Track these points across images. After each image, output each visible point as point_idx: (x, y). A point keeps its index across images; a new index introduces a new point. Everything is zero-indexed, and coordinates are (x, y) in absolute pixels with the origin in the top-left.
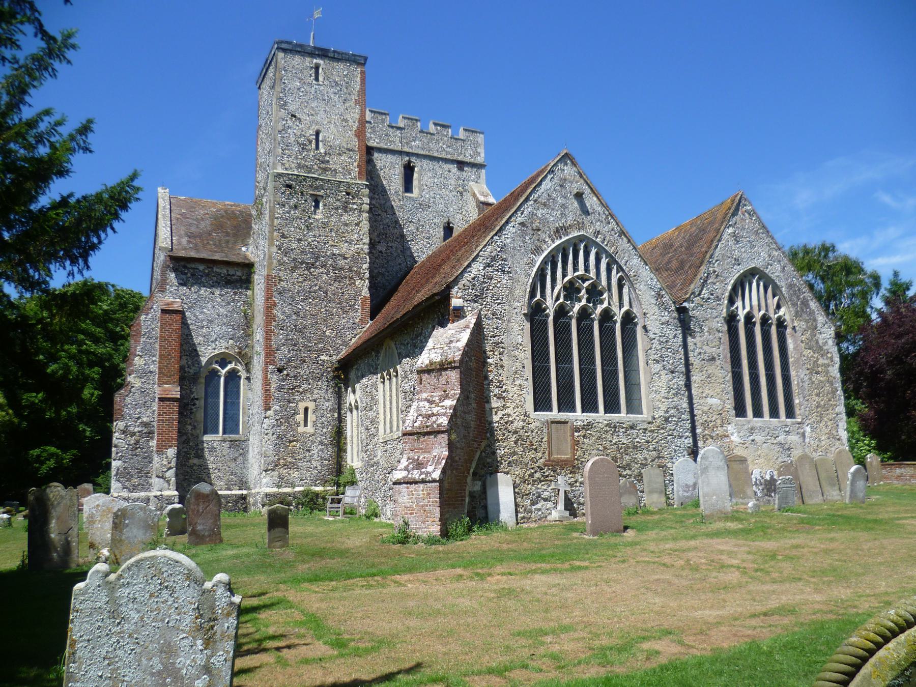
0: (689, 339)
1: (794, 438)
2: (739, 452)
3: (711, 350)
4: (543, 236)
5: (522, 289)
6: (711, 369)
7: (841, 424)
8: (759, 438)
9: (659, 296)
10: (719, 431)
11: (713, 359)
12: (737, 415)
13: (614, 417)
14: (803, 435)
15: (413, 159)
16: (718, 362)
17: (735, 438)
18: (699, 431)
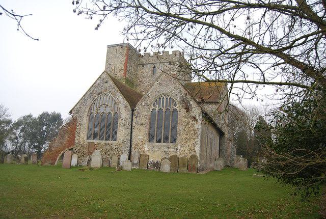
0: (134, 119)
1: (172, 150)
2: (147, 153)
3: (142, 121)
4: (96, 95)
5: (87, 110)
6: (140, 127)
7: (196, 146)
8: (156, 149)
9: (126, 107)
10: (141, 146)
11: (142, 124)
12: (149, 141)
13: (107, 142)
14: (177, 149)
15: (156, 65)
16: (144, 125)
17: (146, 149)
18: (133, 146)
